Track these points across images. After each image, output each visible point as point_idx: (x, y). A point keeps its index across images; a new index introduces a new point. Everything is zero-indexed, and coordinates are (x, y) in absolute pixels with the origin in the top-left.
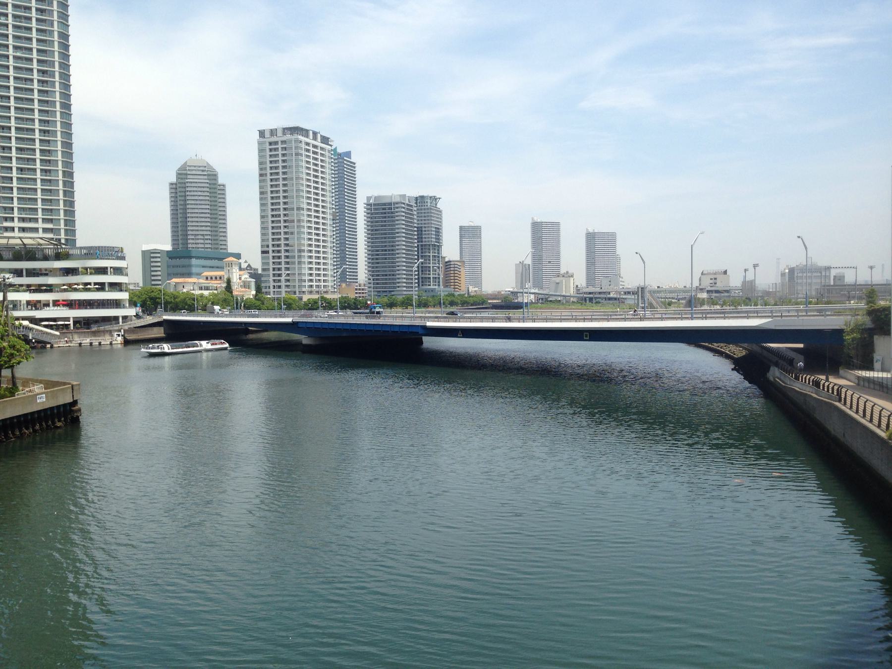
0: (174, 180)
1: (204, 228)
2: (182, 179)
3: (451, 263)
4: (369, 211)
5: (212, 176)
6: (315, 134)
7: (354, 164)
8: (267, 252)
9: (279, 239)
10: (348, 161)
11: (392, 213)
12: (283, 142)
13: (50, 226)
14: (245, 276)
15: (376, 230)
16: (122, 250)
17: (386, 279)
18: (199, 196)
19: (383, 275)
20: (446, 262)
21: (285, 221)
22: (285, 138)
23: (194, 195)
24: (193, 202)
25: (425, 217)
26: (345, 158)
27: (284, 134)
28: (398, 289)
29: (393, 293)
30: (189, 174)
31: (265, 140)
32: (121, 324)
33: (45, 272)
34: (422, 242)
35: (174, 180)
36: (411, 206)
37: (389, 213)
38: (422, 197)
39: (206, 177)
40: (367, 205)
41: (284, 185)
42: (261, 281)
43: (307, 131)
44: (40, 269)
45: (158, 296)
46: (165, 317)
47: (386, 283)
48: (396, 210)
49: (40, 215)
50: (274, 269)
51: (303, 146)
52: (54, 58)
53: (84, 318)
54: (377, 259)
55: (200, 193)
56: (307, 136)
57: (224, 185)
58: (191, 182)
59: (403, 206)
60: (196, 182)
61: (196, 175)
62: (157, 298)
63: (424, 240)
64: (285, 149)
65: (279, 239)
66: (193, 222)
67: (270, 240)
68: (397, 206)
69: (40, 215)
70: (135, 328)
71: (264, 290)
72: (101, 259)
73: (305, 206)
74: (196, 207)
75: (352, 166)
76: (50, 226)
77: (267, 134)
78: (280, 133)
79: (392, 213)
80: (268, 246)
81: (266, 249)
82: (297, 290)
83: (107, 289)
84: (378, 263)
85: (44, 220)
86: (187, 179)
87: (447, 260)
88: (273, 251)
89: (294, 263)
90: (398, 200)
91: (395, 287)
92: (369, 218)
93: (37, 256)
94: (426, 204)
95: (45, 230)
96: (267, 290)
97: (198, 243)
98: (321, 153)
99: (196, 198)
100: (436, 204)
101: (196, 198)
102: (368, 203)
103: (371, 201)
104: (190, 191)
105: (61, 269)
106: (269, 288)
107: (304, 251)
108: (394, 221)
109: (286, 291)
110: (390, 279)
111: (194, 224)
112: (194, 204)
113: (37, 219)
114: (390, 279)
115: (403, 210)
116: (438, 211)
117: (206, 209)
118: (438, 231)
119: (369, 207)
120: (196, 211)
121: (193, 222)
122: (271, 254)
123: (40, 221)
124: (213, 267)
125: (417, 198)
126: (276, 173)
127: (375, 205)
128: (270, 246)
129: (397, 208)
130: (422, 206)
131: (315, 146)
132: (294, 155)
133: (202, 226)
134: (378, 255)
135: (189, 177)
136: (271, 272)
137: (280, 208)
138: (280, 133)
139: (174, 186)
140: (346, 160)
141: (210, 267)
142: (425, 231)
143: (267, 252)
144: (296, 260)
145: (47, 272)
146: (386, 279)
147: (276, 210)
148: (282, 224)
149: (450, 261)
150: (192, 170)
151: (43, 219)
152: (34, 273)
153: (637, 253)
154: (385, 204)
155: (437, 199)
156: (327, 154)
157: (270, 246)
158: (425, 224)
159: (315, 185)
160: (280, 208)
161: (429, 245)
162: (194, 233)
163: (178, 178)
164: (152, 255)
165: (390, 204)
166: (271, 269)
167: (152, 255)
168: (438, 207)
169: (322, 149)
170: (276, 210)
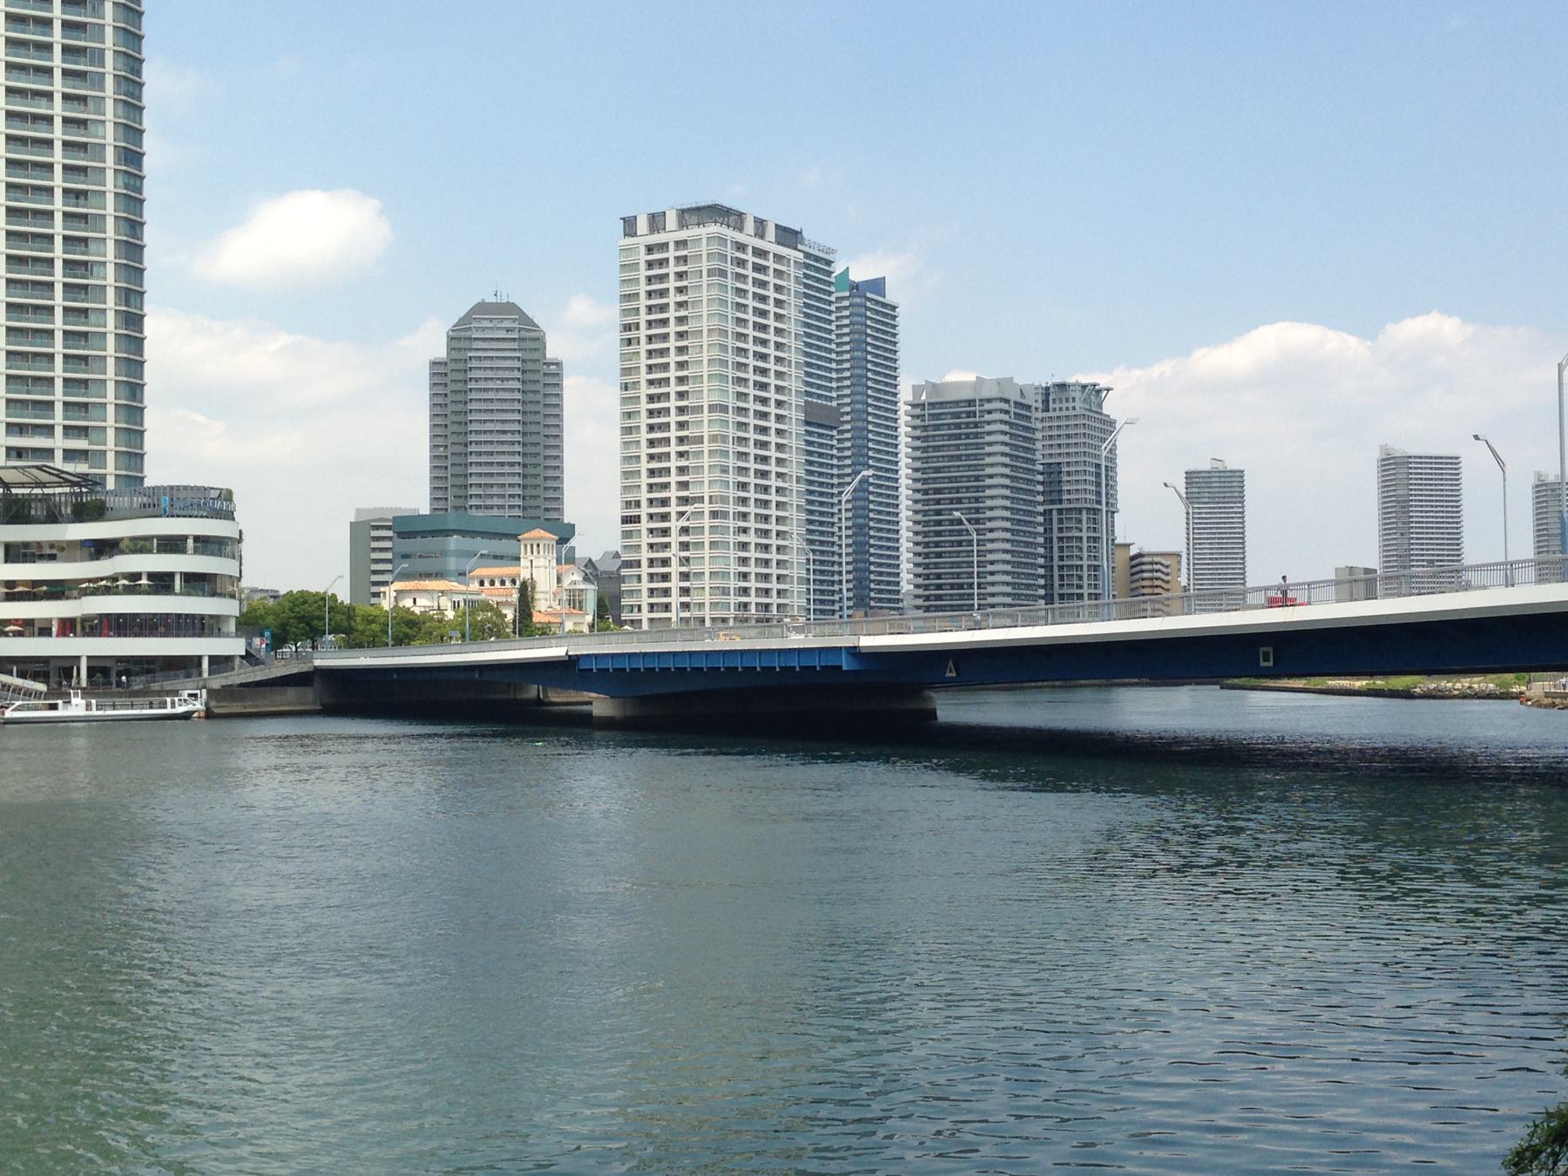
0: (441, 353)
2: (460, 350)
3: (1145, 560)
4: (918, 422)
6: (760, 224)
7: (894, 308)
8: (636, 519)
9: (666, 486)
10: (877, 302)
11: (976, 425)
12: (681, 244)
13: (81, 444)
14: (574, 577)
15: (937, 470)
16: (228, 496)
18: (497, 390)
19: (952, 586)
20: (1133, 558)
21: (681, 440)
22: (683, 235)
23: (486, 390)
24: (483, 406)
25: (1068, 436)
26: (869, 295)
27: (682, 225)
30: (476, 339)
32: (205, 675)
33: (49, 552)
34: (1061, 501)
35: (441, 353)
36: (1028, 407)
37: (967, 425)
38: (1062, 387)
40: (914, 406)
41: (681, 350)
42: (618, 597)
43: (741, 215)
44: (39, 544)
45: (316, 614)
46: (317, 663)
48: (987, 417)
49: (59, 418)
50: (651, 562)
51: (730, 252)
52: (103, 43)
53: (119, 659)
54: (937, 544)
55: (498, 384)
57: (558, 364)
59: (1006, 407)
61: (492, 339)
62: (314, 618)
63: (1065, 497)
65: (666, 486)
66: (480, 454)
67: (644, 488)
68: (987, 406)
69: (59, 418)
70: (242, 685)
71: (625, 616)
72: (173, 516)
73: (732, 402)
75: (886, 315)
76: (81, 444)
77: (642, 225)
78: (671, 221)
79: (976, 425)
80: (638, 504)
81: (633, 512)
83: (177, 587)
84: (939, 555)
86: (470, 350)
87: (1133, 551)
88: (651, 516)
89: (700, 545)
90: (995, 393)
92: (918, 438)
93: (33, 512)
94: (1071, 405)
96: (635, 616)
97: (491, 507)
98: (775, 270)
99: (491, 395)
100: (1100, 405)
102: (917, 402)
103: (923, 397)
104: (477, 380)
105: (84, 544)
106: (639, 610)
107: (725, 515)
108: (978, 446)
111: (483, 459)
112: (485, 411)
113: (52, 427)
115: (1006, 417)
116: (1104, 422)
118: (1103, 476)
119: (918, 411)
120: (489, 427)
121: (480, 454)
122: (645, 524)
123: (59, 431)
124: (502, 557)
125: (1047, 389)
126: (661, 320)
127: (932, 405)
128: (644, 503)
129: (989, 412)
130: (1061, 409)
131: (761, 253)
132: (705, 273)
133: (502, 464)
134: (938, 534)
135: (476, 345)
136: (645, 570)
137: (669, 409)
138: (671, 221)
140: (870, 300)
141: (496, 557)
142: (1069, 473)
143: (636, 519)
145: (54, 551)
147: (659, 412)
148: (673, 448)
149: (1140, 555)
150: (483, 329)
151: (65, 427)
152: (25, 555)
153: (1476, 437)
154: (957, 403)
155: (1099, 392)
156: (792, 270)
157: (644, 503)
158: (1068, 454)
159: (760, 349)
160: (669, 409)
161: (1080, 511)
163: (450, 349)
165: (971, 402)
166: (645, 563)
168: (1104, 412)
169: (779, 258)
170: (659, 412)
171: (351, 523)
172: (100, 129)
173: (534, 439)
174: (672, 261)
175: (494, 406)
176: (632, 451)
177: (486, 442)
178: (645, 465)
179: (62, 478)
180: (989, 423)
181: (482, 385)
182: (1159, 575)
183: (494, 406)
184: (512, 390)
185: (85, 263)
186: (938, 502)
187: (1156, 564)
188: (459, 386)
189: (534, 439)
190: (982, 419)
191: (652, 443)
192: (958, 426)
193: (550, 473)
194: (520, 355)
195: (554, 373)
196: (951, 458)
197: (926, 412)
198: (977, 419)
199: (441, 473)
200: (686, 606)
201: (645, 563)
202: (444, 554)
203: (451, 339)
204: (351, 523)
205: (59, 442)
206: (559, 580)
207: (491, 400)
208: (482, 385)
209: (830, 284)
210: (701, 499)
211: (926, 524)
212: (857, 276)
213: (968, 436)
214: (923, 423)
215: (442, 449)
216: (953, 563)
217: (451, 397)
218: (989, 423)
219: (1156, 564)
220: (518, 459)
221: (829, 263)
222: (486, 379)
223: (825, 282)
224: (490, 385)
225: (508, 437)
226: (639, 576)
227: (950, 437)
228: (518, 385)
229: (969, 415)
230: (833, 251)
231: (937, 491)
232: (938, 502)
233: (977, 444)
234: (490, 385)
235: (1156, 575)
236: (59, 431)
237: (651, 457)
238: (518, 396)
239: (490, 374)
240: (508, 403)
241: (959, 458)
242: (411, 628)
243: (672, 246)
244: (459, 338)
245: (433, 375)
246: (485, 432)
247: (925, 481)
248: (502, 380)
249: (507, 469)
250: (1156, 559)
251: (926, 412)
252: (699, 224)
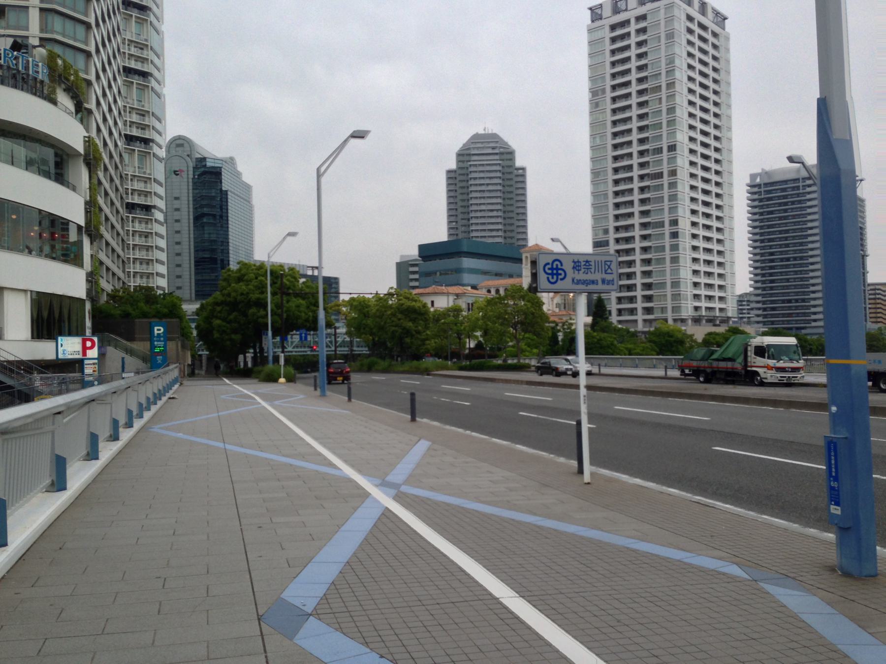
0: (453, 165)
1: (494, 234)
5: (508, 154)
9: (630, 215)
11: (798, 195)
12: (642, 18)
17: (790, 308)
18: (488, 184)
22: (642, 10)
23: (481, 185)
24: (478, 195)
28: (814, 324)
29: (804, 331)
35: (453, 165)
39: (497, 157)
45: (254, 296)
47: (790, 315)
48: (808, 189)
55: (488, 181)
57: (523, 169)
58: (475, 165)
60: (483, 165)
62: (249, 304)
64: (643, 31)
66: (477, 224)
74: (482, 201)
79: (798, 195)
80: (606, 231)
82: (670, 315)
84: (772, 281)
86: (470, 161)
91: (809, 322)
99: (483, 188)
101: (483, 188)
104: (475, 179)
109: (645, 321)
110: (797, 308)
114: (797, 308)
117: (497, 204)
119: (756, 190)
120: (483, 207)
127: (766, 185)
139: (452, 175)
144: (668, 254)
146: (790, 308)
154: (785, 182)
163: (458, 161)
164: (411, 269)
165: (796, 180)
167: (411, 269)
171: (397, 263)
173: (510, 215)
175: (487, 194)
176: (602, 188)
177: (481, 217)
178: (612, 200)
180: (809, 193)
181: (478, 182)
182: (880, 296)
183: (487, 194)
184: (496, 184)
186: (771, 247)
187: (878, 289)
188: (464, 184)
189: (510, 215)
190: (804, 191)
191: (616, 182)
192: (785, 197)
193: (520, 236)
194: (501, 162)
195: (521, 174)
196: (780, 218)
197: (762, 190)
198: (801, 191)
199: (454, 213)
200: (648, 311)
202: (459, 271)
203: (459, 155)
204: (397, 263)
207: (483, 191)
208: (478, 182)
210: (661, 224)
211: (763, 261)
213: (793, 203)
214: (760, 197)
215: (454, 223)
216: (784, 286)
217: (460, 191)
218: (809, 193)
219: (878, 289)
220: (500, 227)
222: (480, 178)
224: (482, 182)
225: (495, 214)
227: (780, 204)
228: (500, 181)
229: (793, 188)
231: (770, 240)
232: (771, 247)
233: (801, 207)
234: (482, 182)
235: (877, 296)
237: (617, 194)
238: (499, 188)
239: (482, 175)
240: (495, 179)
241: (785, 218)
242: (413, 320)
243: (633, 21)
244: (463, 155)
245: (448, 178)
246: (481, 211)
247: (761, 234)
248: (490, 178)
249: (494, 234)
250: (877, 287)
251: (762, 190)
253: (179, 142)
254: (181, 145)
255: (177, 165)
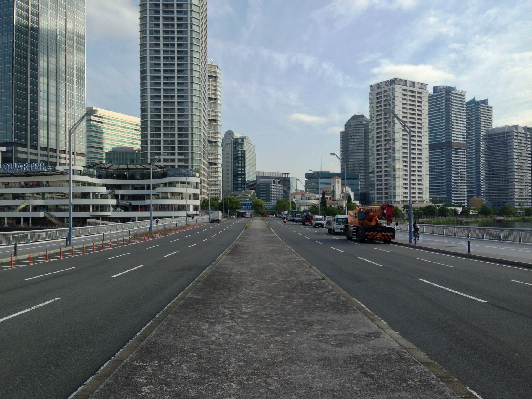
6: (413, 84)
7: (491, 108)
21: (385, 149)
26: (481, 104)
31: (374, 92)
49: (176, 151)
56: (406, 85)
68: (509, 134)
69: (176, 151)
77: (375, 88)
85: (179, 154)
95: (179, 160)
123: (176, 154)
128: (375, 168)
135: (352, 127)
154: (499, 134)
162: (353, 163)
163: (345, 128)
165: (504, 133)
166: (376, 185)
172: (187, 71)
174: (383, 97)
179: (160, 167)
185: (183, 109)
201: (376, 185)
203: (345, 125)
205: (176, 157)
206: (342, 191)
209: (464, 102)
212: (477, 99)
221: (464, 96)
223: (462, 101)
226: (374, 189)
229: (503, 137)
230: (466, 92)
236: (176, 154)
252: (390, 85)
253: (229, 133)
254: (230, 134)
255: (228, 141)
